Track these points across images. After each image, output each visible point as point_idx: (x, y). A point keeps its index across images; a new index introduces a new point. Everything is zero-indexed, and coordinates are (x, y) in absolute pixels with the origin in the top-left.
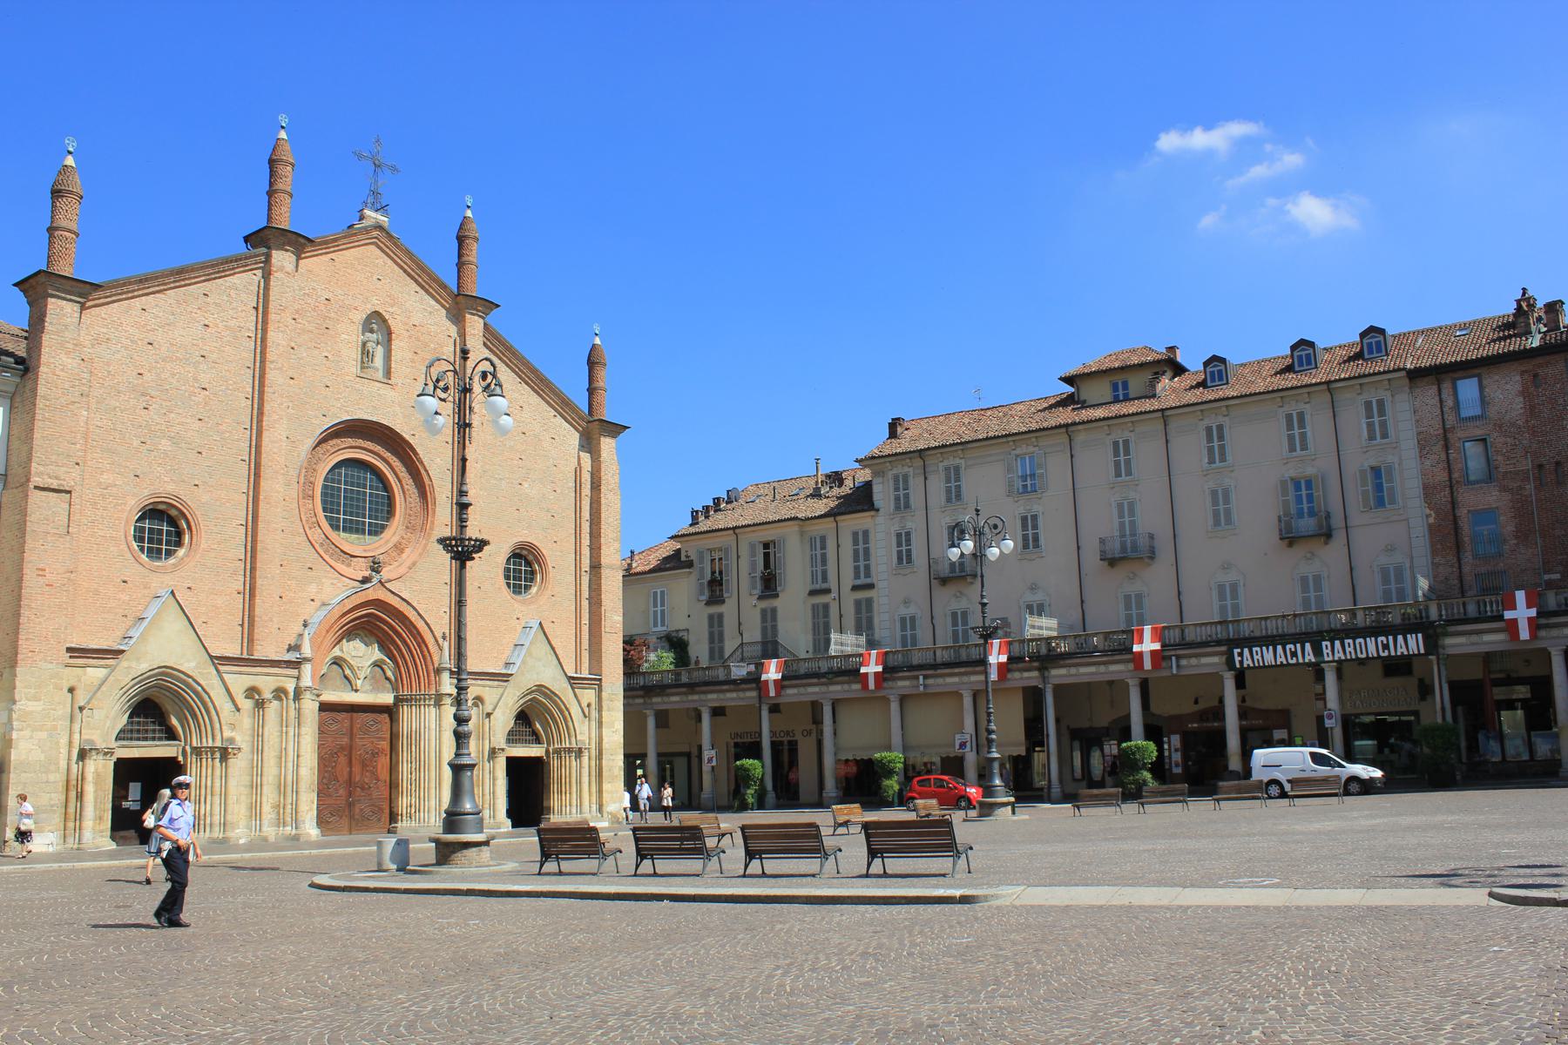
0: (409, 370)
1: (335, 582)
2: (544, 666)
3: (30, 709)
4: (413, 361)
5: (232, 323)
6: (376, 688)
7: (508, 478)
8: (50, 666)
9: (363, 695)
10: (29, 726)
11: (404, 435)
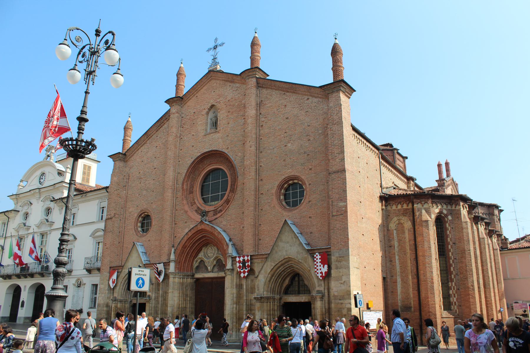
2: (291, 246)
4: (227, 116)
7: (278, 146)
9: (213, 273)
11: (223, 150)
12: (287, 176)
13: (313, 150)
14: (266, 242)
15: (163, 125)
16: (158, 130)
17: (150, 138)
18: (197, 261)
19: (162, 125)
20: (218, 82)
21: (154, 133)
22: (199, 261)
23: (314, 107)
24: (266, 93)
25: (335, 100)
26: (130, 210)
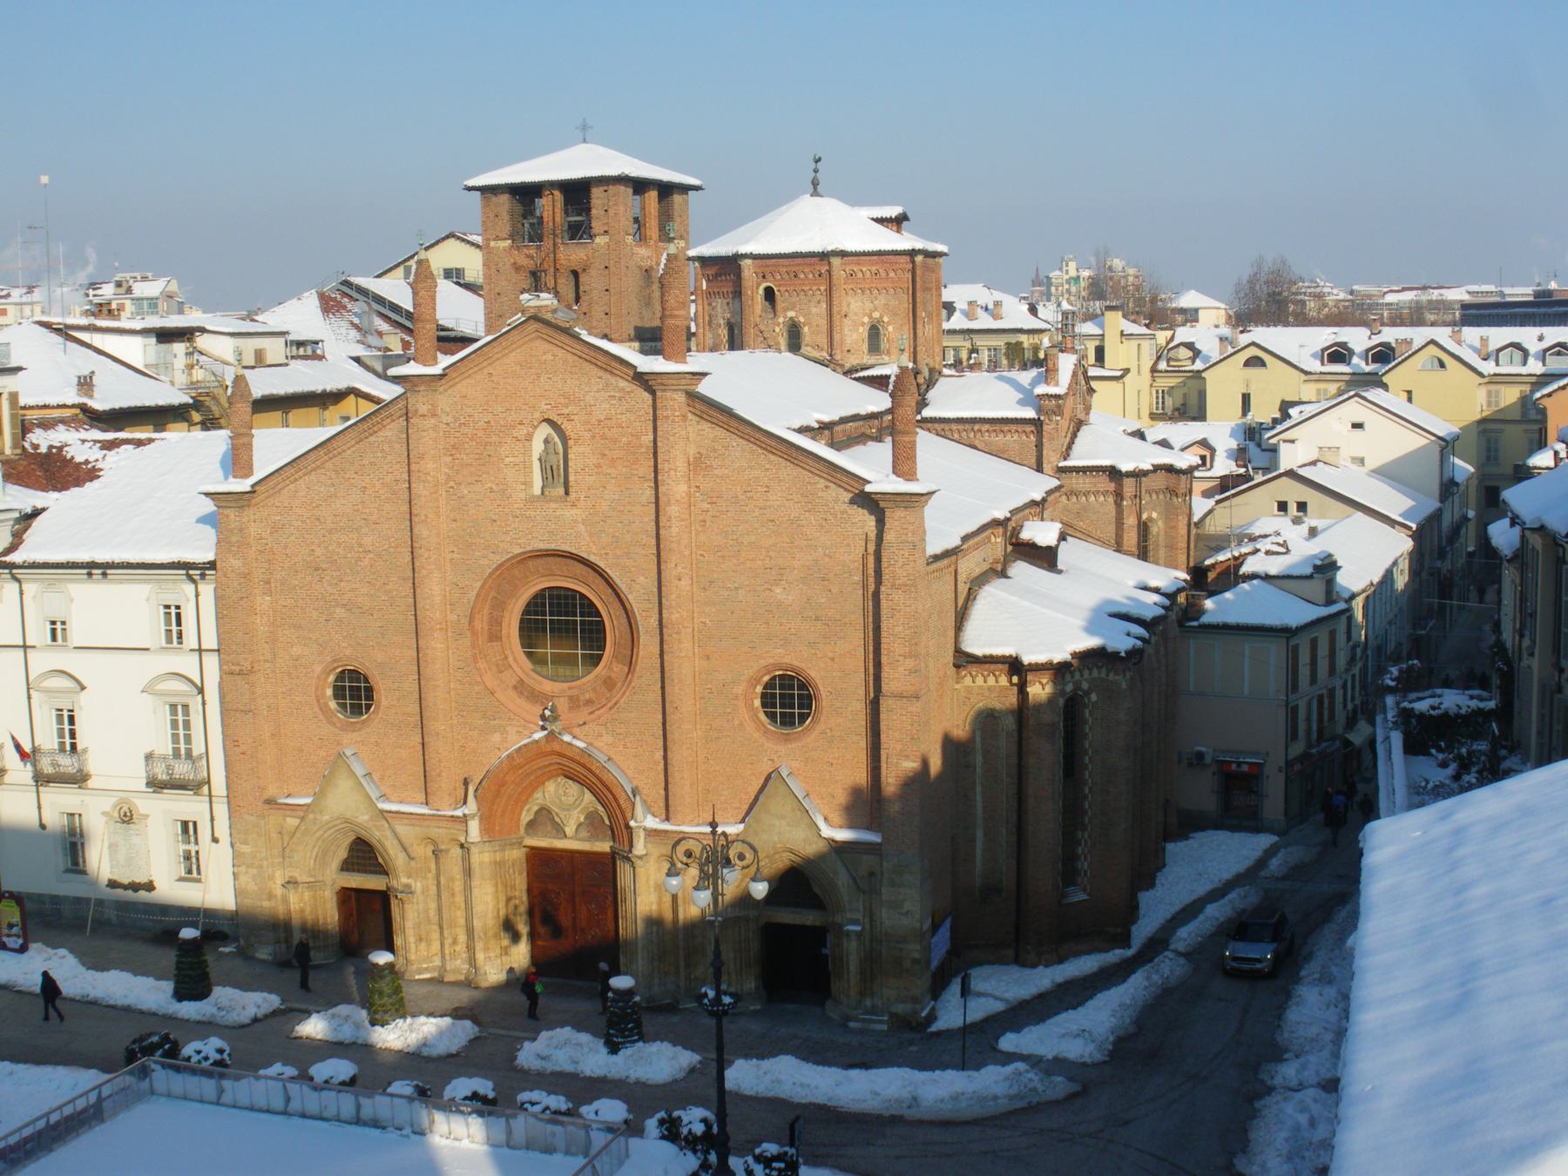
0: (593, 478)
1: (521, 729)
4: (598, 466)
5: (389, 479)
6: (593, 837)
7: (748, 585)
12: (771, 661)
13: (838, 617)
14: (723, 798)
15: (380, 429)
16: (361, 440)
17: (335, 456)
18: (528, 810)
19: (375, 428)
20: (560, 352)
21: (349, 445)
22: (536, 808)
23: (842, 513)
24: (711, 436)
25: (898, 528)
26: (296, 651)
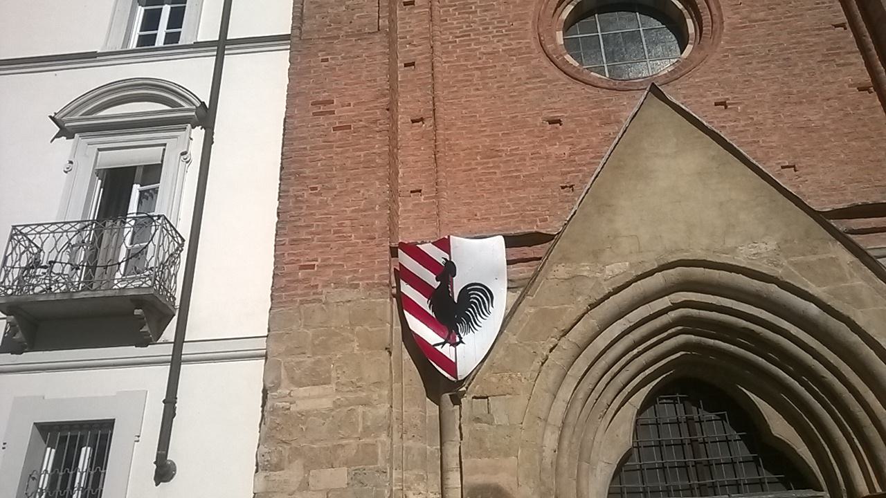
3: (301, 406)
8: (350, 294)
10: (297, 452)
